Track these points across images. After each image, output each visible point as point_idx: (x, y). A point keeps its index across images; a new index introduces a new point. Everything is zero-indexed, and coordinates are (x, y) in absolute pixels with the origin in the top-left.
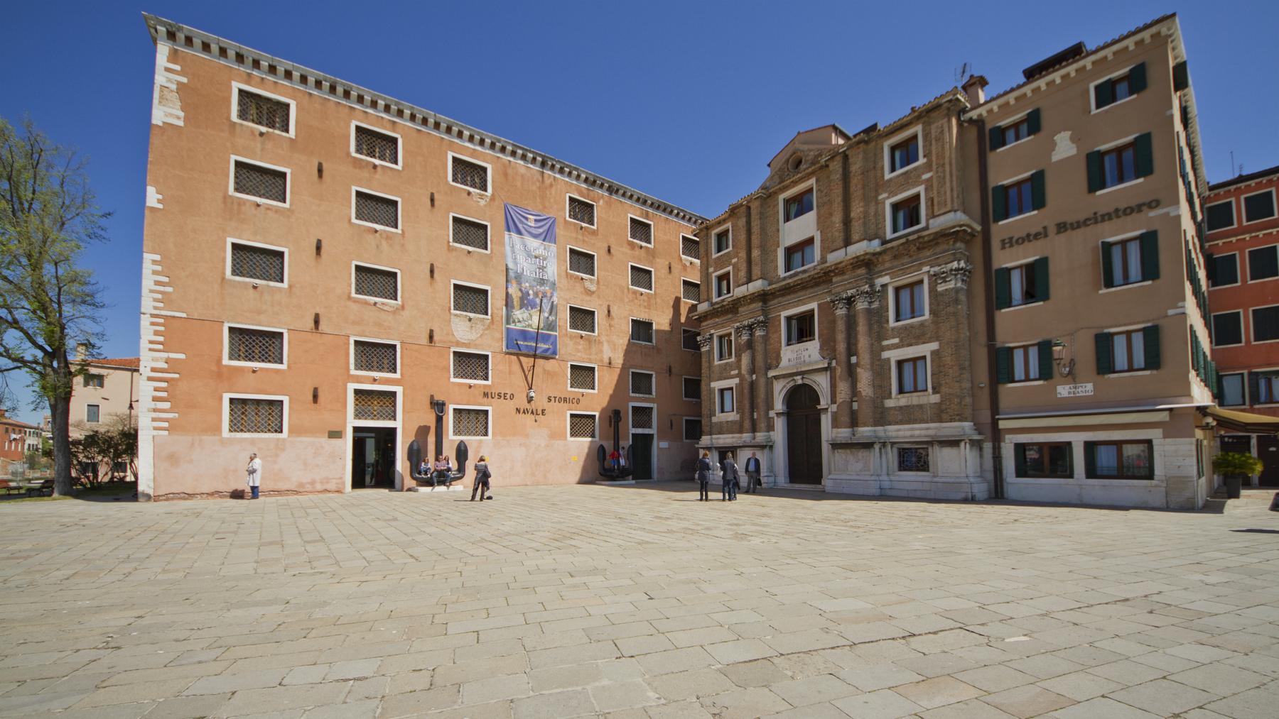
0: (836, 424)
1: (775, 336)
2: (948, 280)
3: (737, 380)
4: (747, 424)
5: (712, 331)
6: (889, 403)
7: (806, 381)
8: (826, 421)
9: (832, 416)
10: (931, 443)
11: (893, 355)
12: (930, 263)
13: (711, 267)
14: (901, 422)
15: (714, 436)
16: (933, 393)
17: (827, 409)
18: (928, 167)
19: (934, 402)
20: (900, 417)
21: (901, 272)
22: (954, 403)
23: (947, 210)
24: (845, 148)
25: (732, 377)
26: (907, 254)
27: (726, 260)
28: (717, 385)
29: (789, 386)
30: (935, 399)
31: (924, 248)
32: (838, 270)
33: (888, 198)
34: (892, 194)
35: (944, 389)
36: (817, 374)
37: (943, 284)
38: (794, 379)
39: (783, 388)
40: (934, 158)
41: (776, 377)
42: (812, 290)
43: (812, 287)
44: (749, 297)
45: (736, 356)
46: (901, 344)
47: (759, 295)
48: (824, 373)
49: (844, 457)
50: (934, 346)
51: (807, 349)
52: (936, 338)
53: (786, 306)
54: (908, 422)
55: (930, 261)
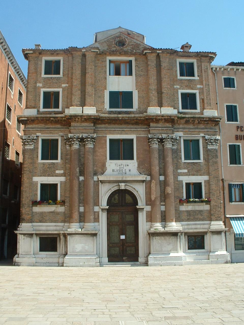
0: (150, 218)
1: (101, 150)
2: (213, 144)
3: (63, 179)
4: (76, 216)
5: (38, 134)
7: (128, 188)
8: (142, 217)
9: (146, 214)
11: (186, 179)
12: (204, 132)
13: (40, 83)
17: (143, 209)
18: (201, 82)
19: (206, 209)
21: (189, 132)
22: (217, 211)
23: (211, 108)
27: (56, 83)
28: (40, 180)
29: (113, 190)
32: (156, 119)
33: (180, 89)
34: (182, 88)
35: (213, 203)
36: (136, 183)
37: (211, 146)
38: (119, 185)
39: (109, 190)
40: (204, 79)
41: (102, 182)
42: (132, 127)
43: (133, 124)
44: (85, 117)
45: (61, 159)
47: (94, 119)
48: (141, 183)
50: (206, 178)
51: (128, 165)
52: (208, 174)
55: (204, 131)
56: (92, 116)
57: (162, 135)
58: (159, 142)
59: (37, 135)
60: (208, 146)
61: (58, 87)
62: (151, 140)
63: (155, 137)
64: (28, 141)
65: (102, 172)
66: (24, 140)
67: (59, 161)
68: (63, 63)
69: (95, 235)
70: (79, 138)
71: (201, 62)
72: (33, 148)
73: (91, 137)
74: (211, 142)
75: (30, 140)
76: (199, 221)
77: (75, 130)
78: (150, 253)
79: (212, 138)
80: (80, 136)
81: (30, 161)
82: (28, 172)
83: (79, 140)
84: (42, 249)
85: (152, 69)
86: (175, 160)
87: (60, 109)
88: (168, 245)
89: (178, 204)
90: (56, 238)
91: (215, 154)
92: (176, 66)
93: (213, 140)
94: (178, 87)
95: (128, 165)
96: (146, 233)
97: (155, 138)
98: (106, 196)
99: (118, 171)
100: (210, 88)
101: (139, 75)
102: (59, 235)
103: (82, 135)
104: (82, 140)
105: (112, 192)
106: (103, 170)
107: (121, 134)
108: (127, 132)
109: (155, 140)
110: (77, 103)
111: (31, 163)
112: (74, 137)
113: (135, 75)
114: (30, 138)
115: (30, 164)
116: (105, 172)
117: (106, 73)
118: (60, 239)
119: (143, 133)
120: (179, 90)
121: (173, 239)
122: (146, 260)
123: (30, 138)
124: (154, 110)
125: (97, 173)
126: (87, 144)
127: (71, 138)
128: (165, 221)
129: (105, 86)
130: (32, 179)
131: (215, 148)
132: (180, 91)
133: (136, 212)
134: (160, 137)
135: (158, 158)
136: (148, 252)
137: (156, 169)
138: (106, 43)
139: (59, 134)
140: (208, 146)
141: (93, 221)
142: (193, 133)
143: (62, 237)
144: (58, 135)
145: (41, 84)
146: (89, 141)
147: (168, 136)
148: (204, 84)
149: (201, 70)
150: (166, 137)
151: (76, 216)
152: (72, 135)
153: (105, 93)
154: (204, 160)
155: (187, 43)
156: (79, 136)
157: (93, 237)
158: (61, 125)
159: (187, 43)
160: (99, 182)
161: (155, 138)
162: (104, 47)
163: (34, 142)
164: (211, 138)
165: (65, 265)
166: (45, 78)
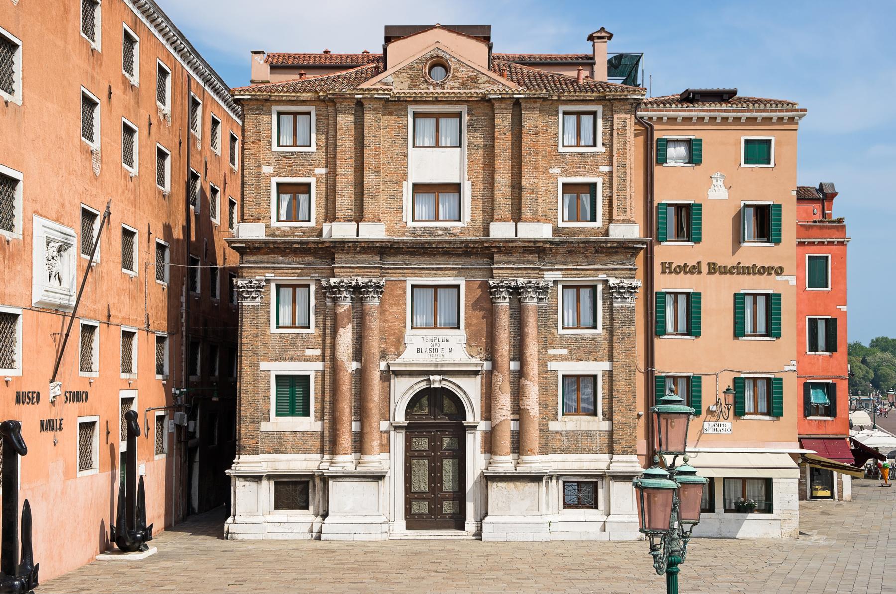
0: (490, 446)
1: (395, 309)
2: (626, 296)
3: (319, 366)
5: (270, 276)
6: (553, 426)
8: (474, 443)
10: (602, 477)
13: (269, 164)
14: (567, 451)
15: (262, 456)
16: (604, 420)
20: (566, 444)
21: (576, 272)
24: (522, 96)
25: (308, 360)
26: (583, 254)
29: (417, 389)
30: (605, 426)
31: (601, 253)
32: (507, 248)
34: (566, 172)
35: (617, 417)
38: (429, 380)
41: (397, 374)
43: (459, 255)
44: (363, 245)
45: (316, 326)
46: (569, 357)
47: (381, 248)
49: (506, 493)
50: (606, 366)
51: (447, 340)
53: (416, 272)
54: (576, 451)
56: (377, 242)
57: (516, 281)
58: (510, 294)
59: (267, 278)
60: (614, 300)
61: (307, 175)
62: (494, 290)
63: (504, 284)
64: (249, 290)
65: (396, 353)
66: (241, 288)
67: (312, 330)
68: (317, 120)
69: (379, 477)
70: (351, 287)
71: (612, 111)
72: (259, 304)
73: (375, 283)
74: (621, 293)
75: (254, 288)
76: (588, 453)
77: (343, 270)
78: (486, 515)
79: (623, 284)
80: (354, 283)
81: (254, 331)
82: (250, 354)
83: (351, 290)
84: (280, 504)
85: (503, 136)
86: (543, 329)
87: (312, 223)
88: (522, 500)
89: (545, 418)
90: (308, 482)
91: (628, 317)
92: (557, 123)
93: (624, 288)
94: (559, 171)
95: (447, 340)
96: (478, 473)
97: (502, 286)
98: (404, 400)
99: (428, 351)
100: (628, 172)
101: (475, 146)
102: (312, 476)
103: (357, 280)
104: (357, 290)
105: (415, 392)
106: (397, 349)
107: (435, 275)
108: (447, 272)
109: (502, 292)
110: (347, 214)
111: (257, 335)
112: (342, 284)
113: (468, 146)
114: (253, 284)
115: (254, 337)
116: (402, 352)
117: (406, 145)
118: (314, 486)
119: (480, 273)
120: (559, 178)
121: (531, 487)
122: (479, 528)
123: (253, 284)
124: (501, 231)
125: (387, 355)
126: (367, 297)
127: (335, 287)
128: (518, 452)
129: (403, 173)
130: (258, 366)
131: (629, 305)
132: (562, 180)
133: (460, 432)
134: (513, 284)
135: (507, 326)
136: (484, 512)
137: (504, 348)
138: (407, 72)
139: (312, 275)
140: (614, 300)
141: (378, 450)
142: (583, 272)
143: (317, 481)
144: (309, 278)
145: (272, 168)
146: (371, 292)
147: (530, 282)
148: (615, 164)
149: (612, 130)
150: (525, 284)
151: (346, 440)
152: (337, 280)
153: (404, 189)
154: (605, 330)
155: (603, 29)
156: (351, 283)
157: (377, 483)
158: (315, 258)
159: (603, 29)
160: (391, 374)
161: (502, 287)
162: (402, 82)
163: (260, 292)
164: (621, 284)
165: (323, 537)
166: (278, 153)
